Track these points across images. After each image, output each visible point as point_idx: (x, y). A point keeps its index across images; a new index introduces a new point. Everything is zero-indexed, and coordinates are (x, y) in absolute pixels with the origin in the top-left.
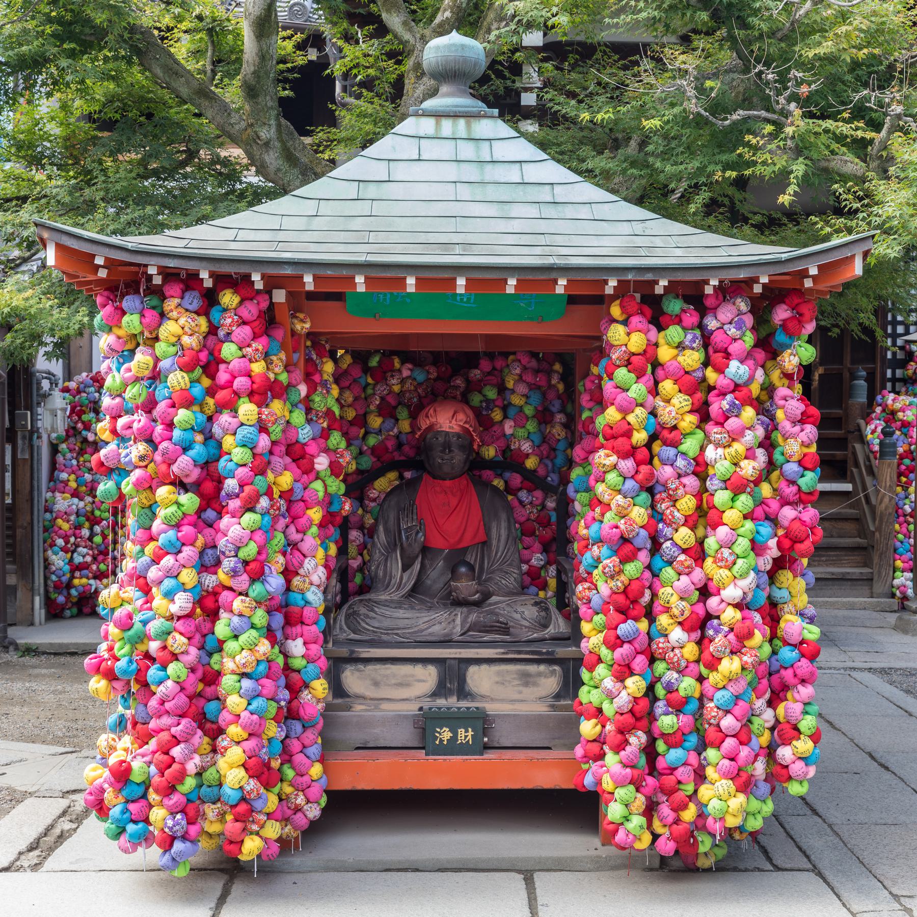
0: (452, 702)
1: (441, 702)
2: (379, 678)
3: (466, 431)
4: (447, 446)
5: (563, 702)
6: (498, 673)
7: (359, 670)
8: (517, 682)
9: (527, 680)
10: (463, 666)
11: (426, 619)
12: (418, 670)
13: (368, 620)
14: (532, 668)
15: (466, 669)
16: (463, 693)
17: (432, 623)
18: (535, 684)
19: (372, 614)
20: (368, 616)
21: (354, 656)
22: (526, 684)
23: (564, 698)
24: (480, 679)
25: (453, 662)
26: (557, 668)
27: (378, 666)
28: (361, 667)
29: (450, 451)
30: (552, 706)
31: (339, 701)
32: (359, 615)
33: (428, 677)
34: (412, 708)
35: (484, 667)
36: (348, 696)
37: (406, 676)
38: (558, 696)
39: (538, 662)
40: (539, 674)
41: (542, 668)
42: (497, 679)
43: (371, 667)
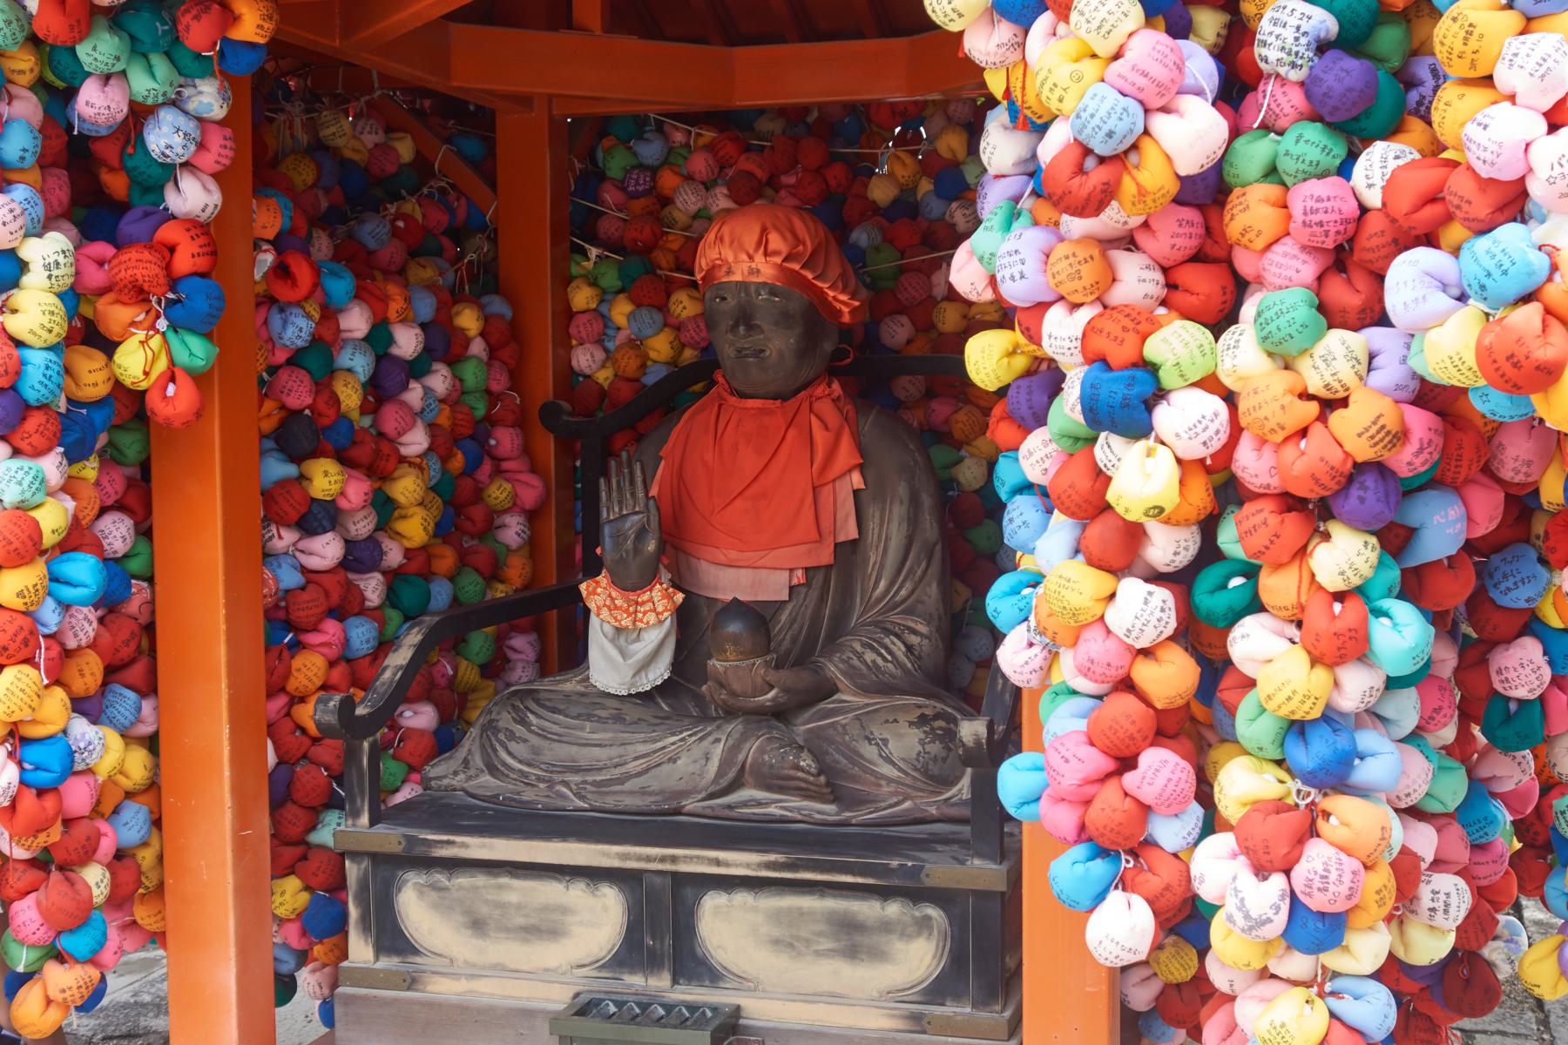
0: (659, 983)
1: (636, 981)
2: (484, 910)
3: (795, 279)
4: (745, 318)
5: (949, 1010)
6: (777, 916)
7: (435, 887)
8: (826, 944)
9: (853, 941)
10: (688, 892)
11: (642, 749)
12: (575, 894)
13: (513, 746)
14: (868, 909)
15: (698, 900)
16: (689, 961)
17: (655, 759)
18: (878, 955)
19: (519, 730)
20: (512, 736)
21: (419, 851)
22: (852, 953)
23: (958, 997)
24: (728, 928)
25: (658, 880)
26: (933, 912)
27: (481, 880)
28: (440, 878)
29: (750, 327)
30: (916, 1018)
31: (388, 963)
32: (496, 731)
33: (599, 919)
34: (558, 997)
35: (742, 898)
36: (415, 951)
37: (546, 908)
38: (938, 990)
39: (885, 893)
40: (886, 927)
41: (894, 909)
42: (777, 933)
43: (463, 881)
